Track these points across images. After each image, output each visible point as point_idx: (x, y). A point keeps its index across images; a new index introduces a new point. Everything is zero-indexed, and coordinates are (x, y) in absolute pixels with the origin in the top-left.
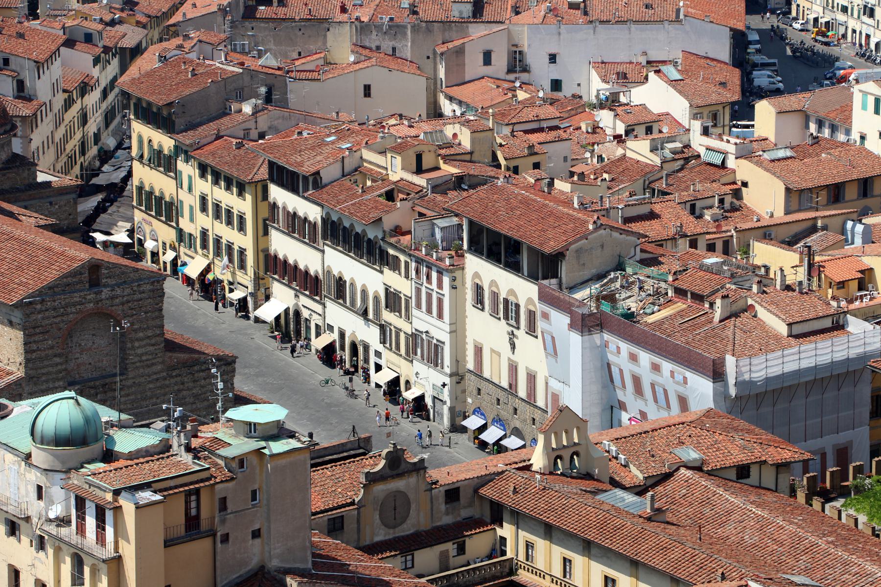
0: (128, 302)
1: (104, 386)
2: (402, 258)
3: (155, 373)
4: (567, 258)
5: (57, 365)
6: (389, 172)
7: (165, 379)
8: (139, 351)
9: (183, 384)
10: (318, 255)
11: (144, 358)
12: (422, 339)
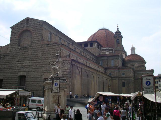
0: (33, 27)
9: (45, 49)
11: (36, 41)
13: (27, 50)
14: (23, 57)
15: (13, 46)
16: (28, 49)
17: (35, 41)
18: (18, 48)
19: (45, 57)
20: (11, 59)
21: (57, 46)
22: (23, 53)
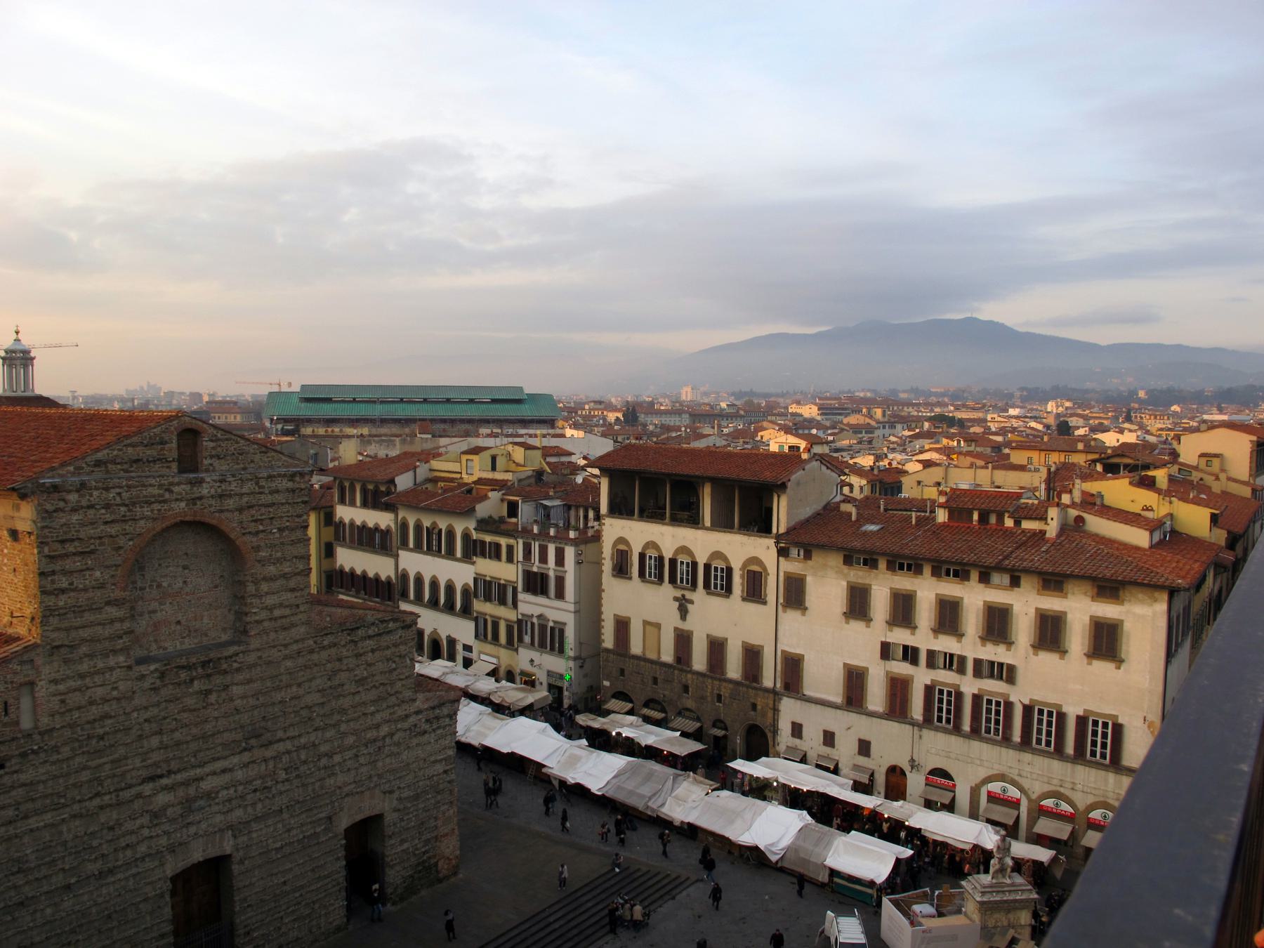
1: (204, 664)
2: (503, 541)
3: (296, 641)
4: (788, 490)
5: (112, 621)
6: (464, 476)
7: (312, 652)
8: (270, 601)
9: (340, 660)
10: (391, 561)
11: (277, 613)
12: (533, 624)
13: (218, 680)
14: (194, 731)
15: (84, 667)
16: (225, 672)
17: (271, 609)
18: (142, 677)
19: (346, 702)
20: (85, 776)
21: (400, 632)
22: (190, 702)
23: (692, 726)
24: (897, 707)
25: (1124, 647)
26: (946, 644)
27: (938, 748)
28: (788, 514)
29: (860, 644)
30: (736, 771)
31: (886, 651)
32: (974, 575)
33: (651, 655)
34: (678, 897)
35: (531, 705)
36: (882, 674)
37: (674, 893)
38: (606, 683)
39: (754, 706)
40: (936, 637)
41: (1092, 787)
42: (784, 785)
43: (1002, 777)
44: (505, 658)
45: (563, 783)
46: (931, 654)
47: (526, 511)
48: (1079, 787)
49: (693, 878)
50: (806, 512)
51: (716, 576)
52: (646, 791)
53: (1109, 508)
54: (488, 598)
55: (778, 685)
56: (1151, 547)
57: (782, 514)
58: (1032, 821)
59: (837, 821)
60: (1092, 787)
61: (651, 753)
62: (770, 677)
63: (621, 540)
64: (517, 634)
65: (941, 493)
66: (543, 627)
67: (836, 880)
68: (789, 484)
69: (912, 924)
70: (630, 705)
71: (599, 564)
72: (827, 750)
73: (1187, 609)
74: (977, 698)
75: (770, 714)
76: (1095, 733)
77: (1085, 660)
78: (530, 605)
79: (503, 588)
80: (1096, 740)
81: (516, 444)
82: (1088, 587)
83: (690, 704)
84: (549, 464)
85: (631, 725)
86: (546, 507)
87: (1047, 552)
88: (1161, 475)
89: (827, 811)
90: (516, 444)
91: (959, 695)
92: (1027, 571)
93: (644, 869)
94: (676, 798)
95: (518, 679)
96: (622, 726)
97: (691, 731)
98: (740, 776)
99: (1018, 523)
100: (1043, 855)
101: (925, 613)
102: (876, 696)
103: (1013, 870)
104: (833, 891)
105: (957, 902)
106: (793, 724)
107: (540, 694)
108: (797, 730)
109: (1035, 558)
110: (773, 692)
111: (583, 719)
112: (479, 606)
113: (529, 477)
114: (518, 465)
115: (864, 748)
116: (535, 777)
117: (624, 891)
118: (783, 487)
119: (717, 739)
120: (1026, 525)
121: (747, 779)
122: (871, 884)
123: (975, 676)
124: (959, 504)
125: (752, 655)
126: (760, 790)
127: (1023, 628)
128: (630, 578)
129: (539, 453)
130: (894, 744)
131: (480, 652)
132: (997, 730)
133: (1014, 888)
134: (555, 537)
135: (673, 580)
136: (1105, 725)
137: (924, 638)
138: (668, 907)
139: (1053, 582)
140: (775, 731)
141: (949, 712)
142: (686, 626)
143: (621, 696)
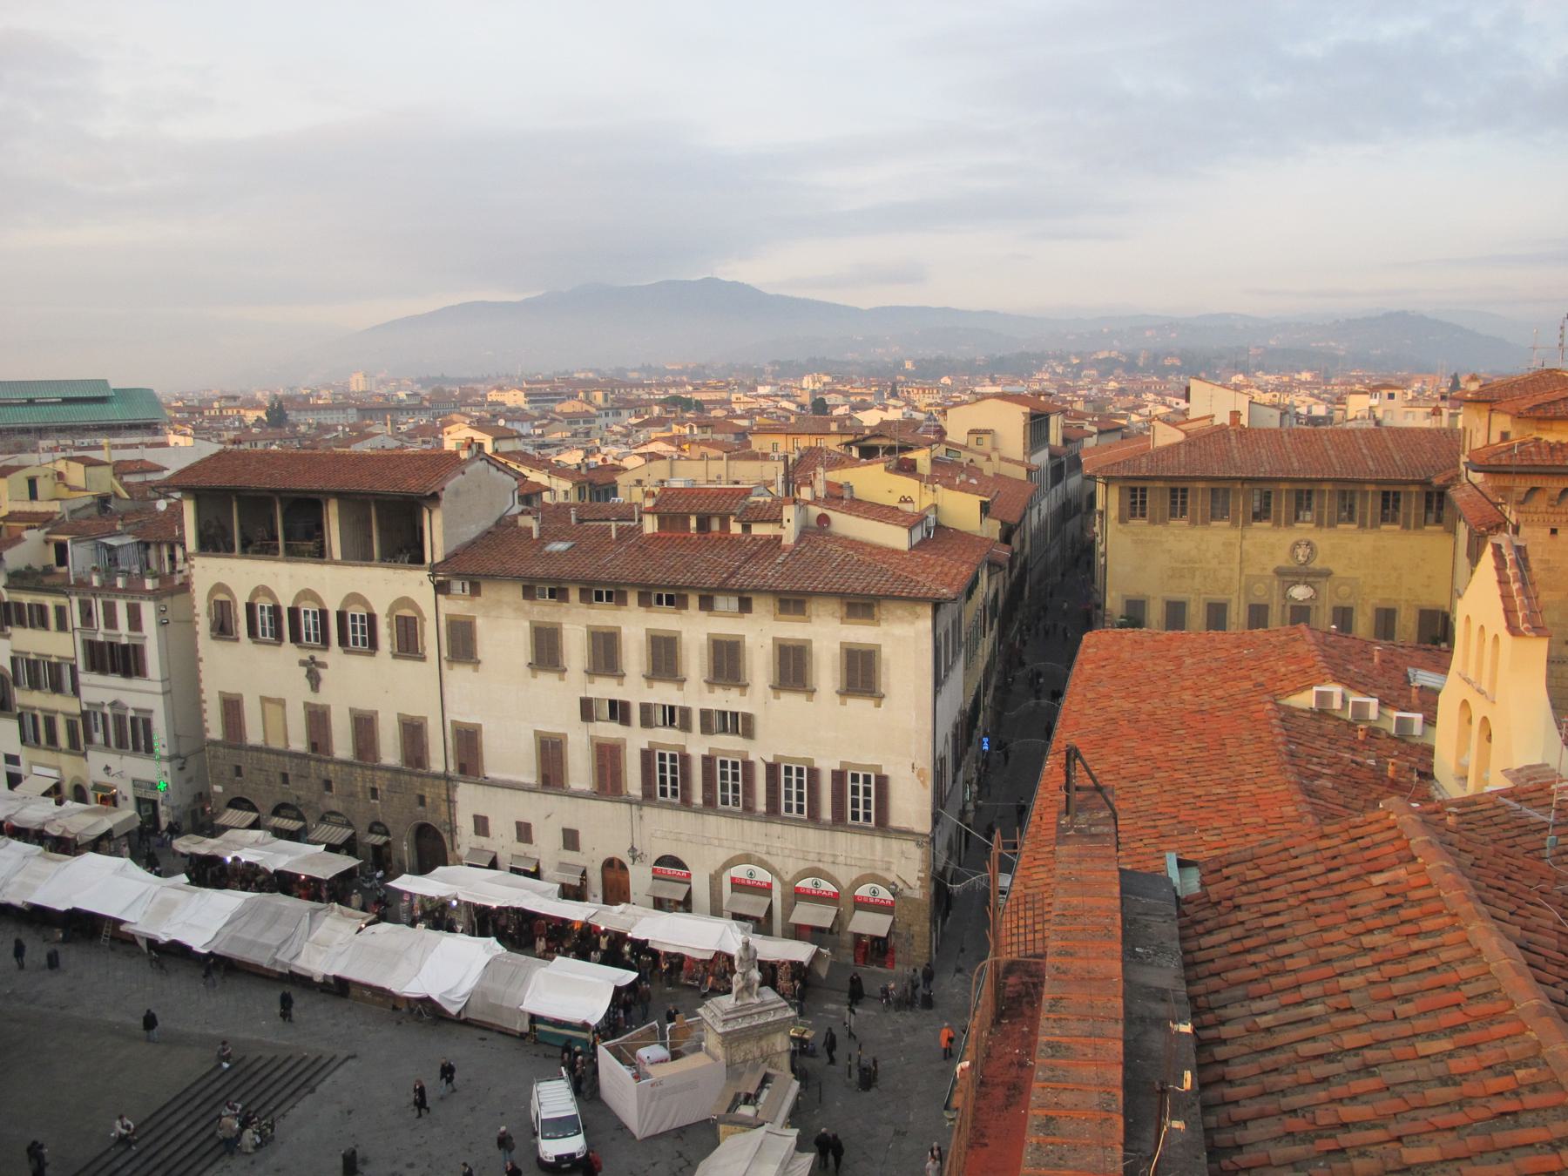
2: (50, 602)
12: (104, 716)
23: (340, 835)
24: (608, 782)
25: (883, 679)
26: (663, 694)
27: (665, 829)
28: (445, 534)
29: (553, 703)
30: (401, 893)
31: (587, 709)
32: (693, 601)
33: (277, 744)
34: (319, 1089)
35: (108, 835)
36: (585, 740)
37: (313, 1082)
38: (218, 788)
39: (422, 800)
40: (650, 687)
41: (850, 857)
42: (468, 904)
43: (746, 859)
44: (69, 768)
45: (152, 943)
46: (646, 709)
47: (81, 557)
48: (841, 859)
49: (343, 1054)
50: (471, 530)
51: (354, 627)
52: (272, 938)
53: (860, 501)
54: (35, 685)
55: (451, 768)
56: (911, 549)
57: (437, 535)
58: (788, 909)
59: (541, 945)
60: (850, 857)
61: (284, 883)
62: (438, 759)
63: (220, 587)
64: (82, 732)
65: (648, 495)
66: (120, 719)
67: (539, 1026)
68: (444, 495)
69: (637, 1077)
70: (254, 816)
71: (191, 622)
72: (523, 848)
73: (957, 623)
74: (708, 761)
75: (444, 807)
76: (855, 790)
77: (838, 699)
78: (101, 689)
79: (55, 669)
80: (858, 800)
81: (71, 459)
82: (834, 606)
83: (334, 804)
84: (127, 486)
85: (256, 844)
86: (110, 548)
87: (783, 564)
88: (922, 457)
89: (522, 932)
90: (71, 459)
91: (686, 759)
92: (758, 591)
93: (270, 1055)
94: (316, 943)
95: (91, 795)
96: (242, 846)
97: (339, 842)
98: (406, 898)
99: (747, 528)
100: (802, 952)
101: (634, 655)
102: (580, 771)
103: (762, 984)
104: (537, 1042)
105: (695, 1034)
106: (476, 818)
107: (126, 813)
108: (481, 826)
109: (769, 573)
110: (446, 777)
111: (183, 845)
112: (23, 697)
113: (86, 506)
114: (72, 489)
115: (571, 839)
116: (112, 938)
117: (235, 1097)
118: (435, 498)
119: (377, 849)
120: (758, 530)
121: (416, 901)
122: (585, 1026)
123: (703, 732)
124: (671, 506)
125: (413, 731)
126: (439, 916)
127: (759, 665)
128: (237, 640)
129: (108, 471)
130: (608, 830)
131: (31, 764)
132: (736, 799)
133: (764, 1008)
134: (125, 590)
135: (296, 638)
136: (867, 779)
137: (635, 689)
138: (307, 1104)
139: (792, 602)
140: (453, 831)
141: (674, 782)
142: (318, 699)
143: (238, 803)
